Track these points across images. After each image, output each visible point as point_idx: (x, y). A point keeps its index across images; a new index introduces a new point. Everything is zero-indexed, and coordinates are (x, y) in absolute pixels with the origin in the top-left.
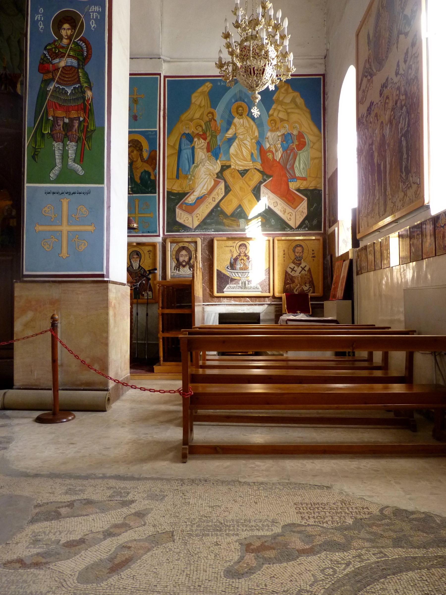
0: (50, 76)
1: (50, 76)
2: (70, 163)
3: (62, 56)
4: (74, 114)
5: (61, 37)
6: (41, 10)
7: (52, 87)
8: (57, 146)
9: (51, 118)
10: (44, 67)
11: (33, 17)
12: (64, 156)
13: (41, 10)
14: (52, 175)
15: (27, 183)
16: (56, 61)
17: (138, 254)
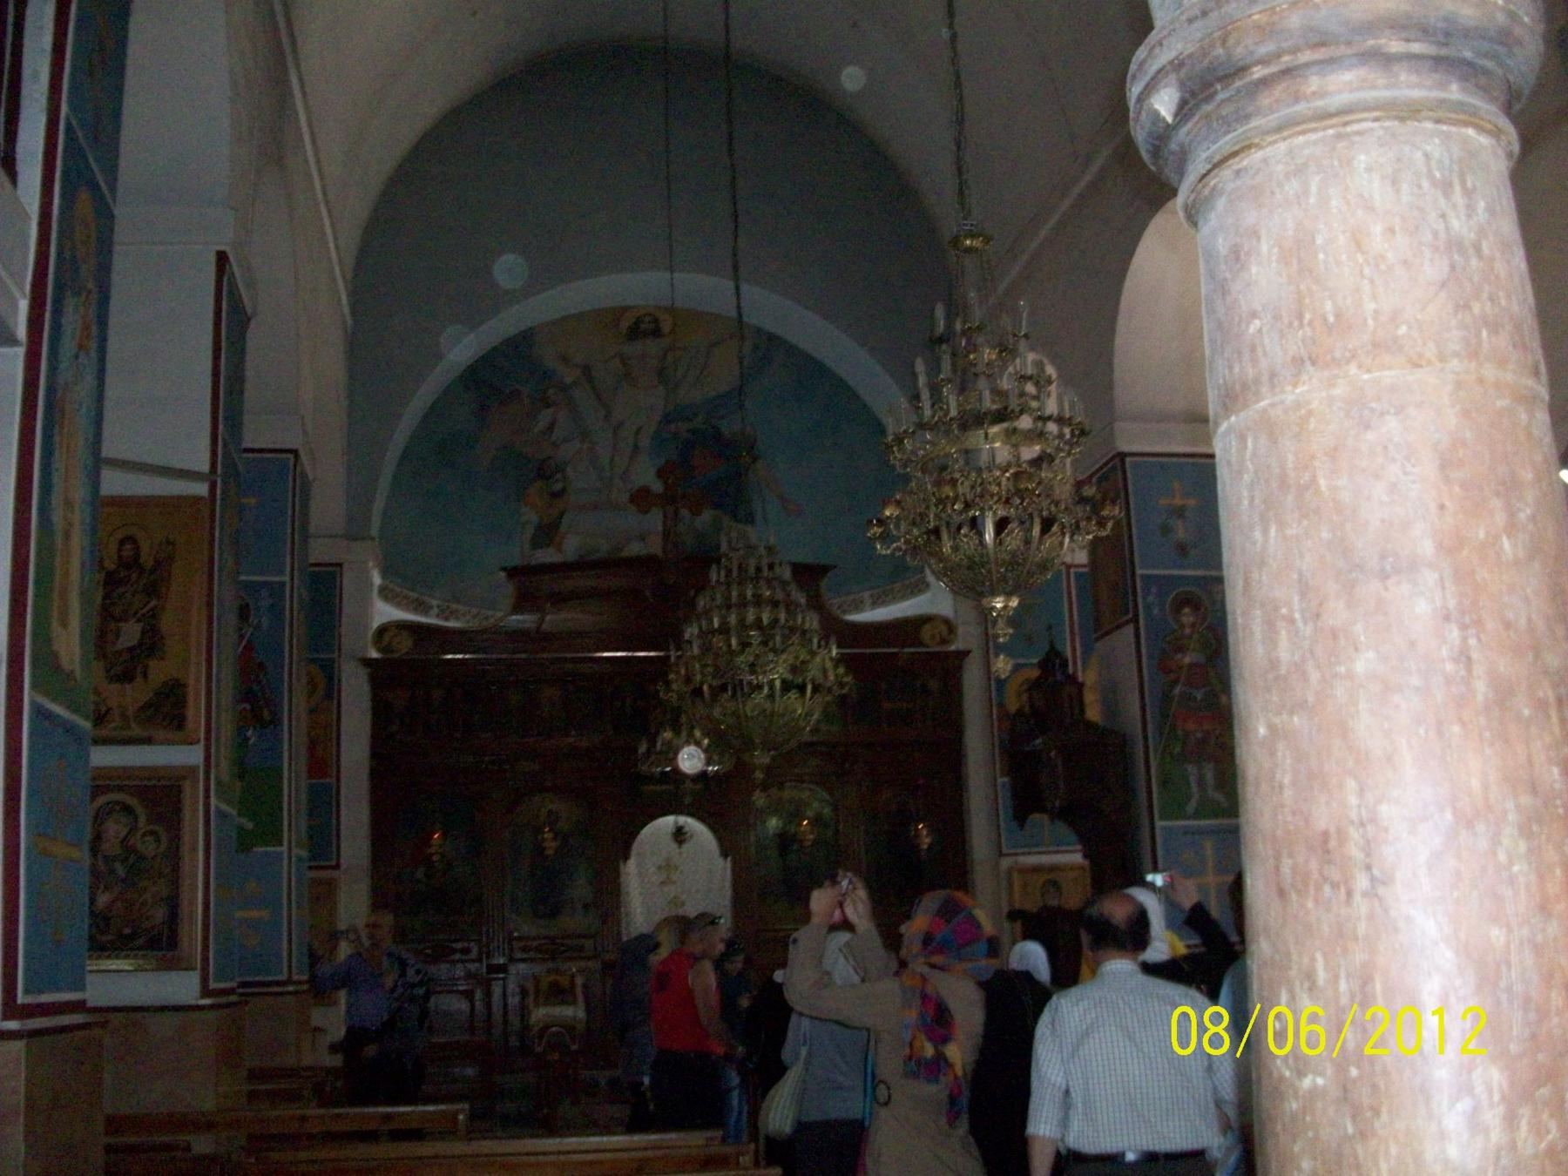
0: (1172, 676)
1: (1172, 676)
2: (1210, 792)
3: (1181, 649)
4: (1206, 727)
5: (1183, 626)
6: (1154, 590)
7: (1177, 690)
8: (1191, 769)
9: (1180, 732)
10: (1163, 666)
11: (1144, 598)
12: (1201, 782)
13: (1154, 590)
14: (1191, 806)
15: (1161, 818)
16: (1179, 656)
17: (1055, 883)
